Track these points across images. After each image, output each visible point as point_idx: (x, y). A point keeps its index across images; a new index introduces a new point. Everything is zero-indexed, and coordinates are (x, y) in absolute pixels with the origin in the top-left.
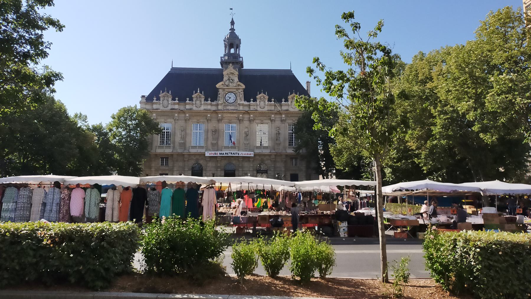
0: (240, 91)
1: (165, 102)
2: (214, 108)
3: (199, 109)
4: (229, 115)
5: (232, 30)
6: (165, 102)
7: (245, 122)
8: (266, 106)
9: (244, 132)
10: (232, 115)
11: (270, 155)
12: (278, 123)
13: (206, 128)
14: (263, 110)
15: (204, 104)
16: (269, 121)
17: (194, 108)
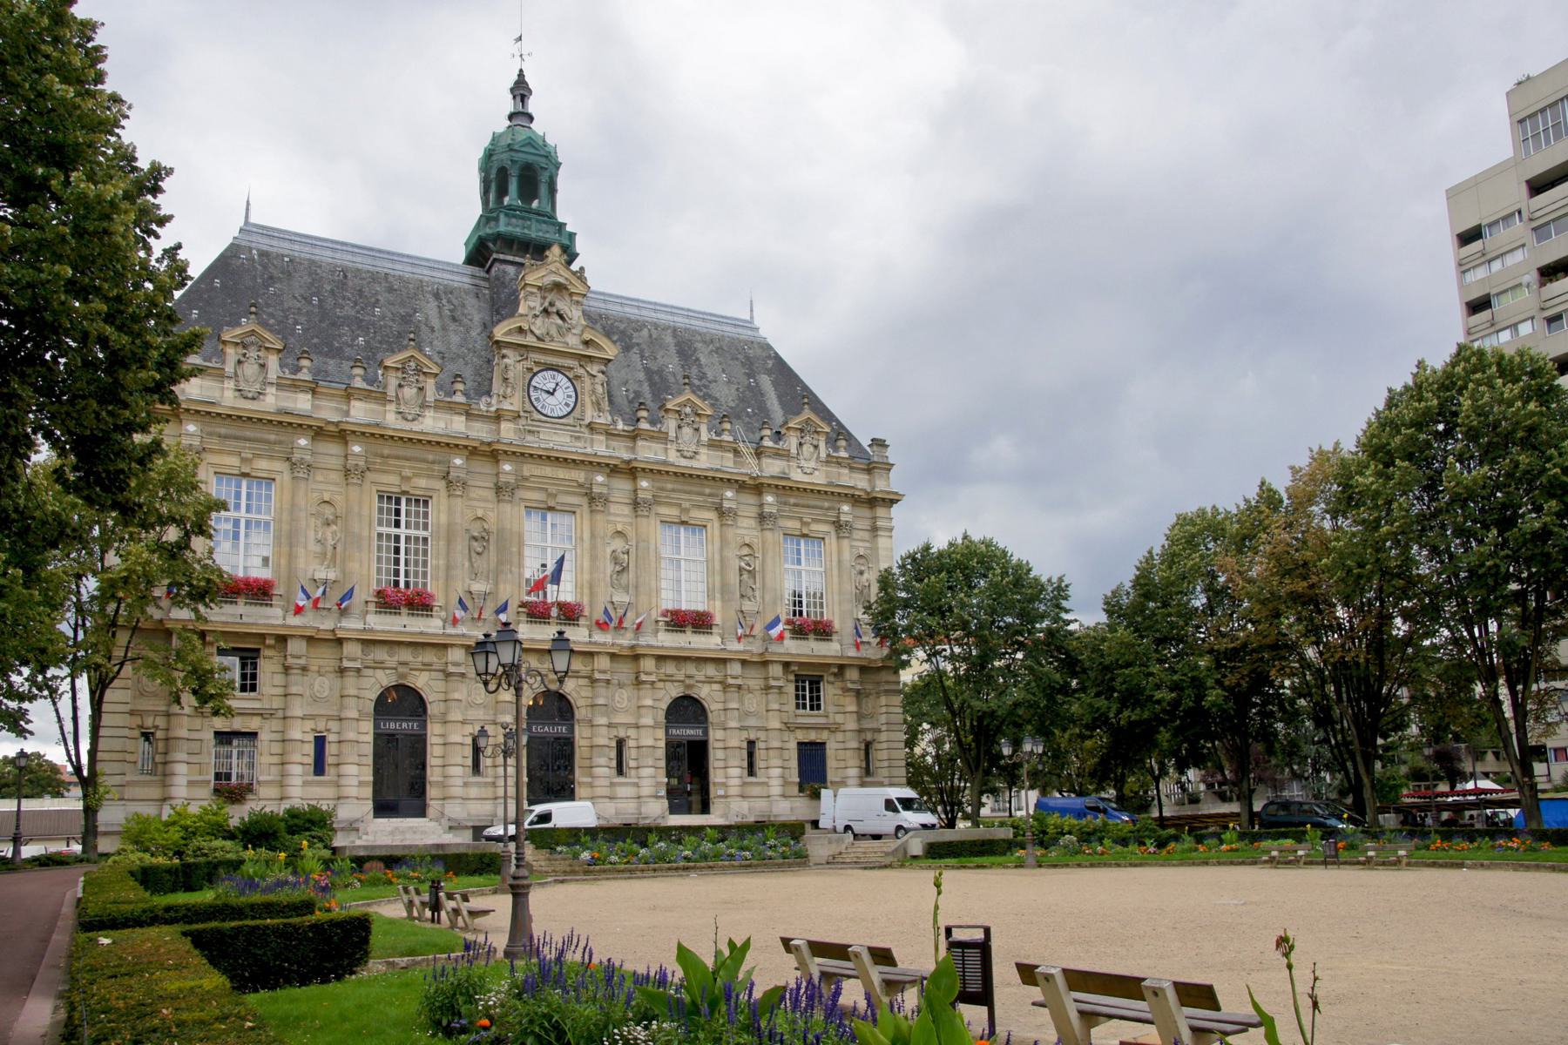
0: (594, 369)
1: (250, 369)
2: (480, 432)
3: (416, 427)
4: (548, 471)
5: (521, 116)
6: (250, 369)
7: (613, 508)
8: (703, 451)
9: (609, 551)
10: (562, 473)
11: (722, 662)
12: (746, 527)
13: (443, 518)
14: (694, 464)
15: (438, 406)
16: (712, 515)
17: (391, 419)
